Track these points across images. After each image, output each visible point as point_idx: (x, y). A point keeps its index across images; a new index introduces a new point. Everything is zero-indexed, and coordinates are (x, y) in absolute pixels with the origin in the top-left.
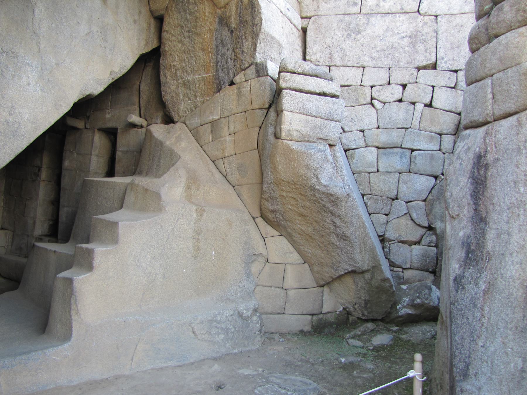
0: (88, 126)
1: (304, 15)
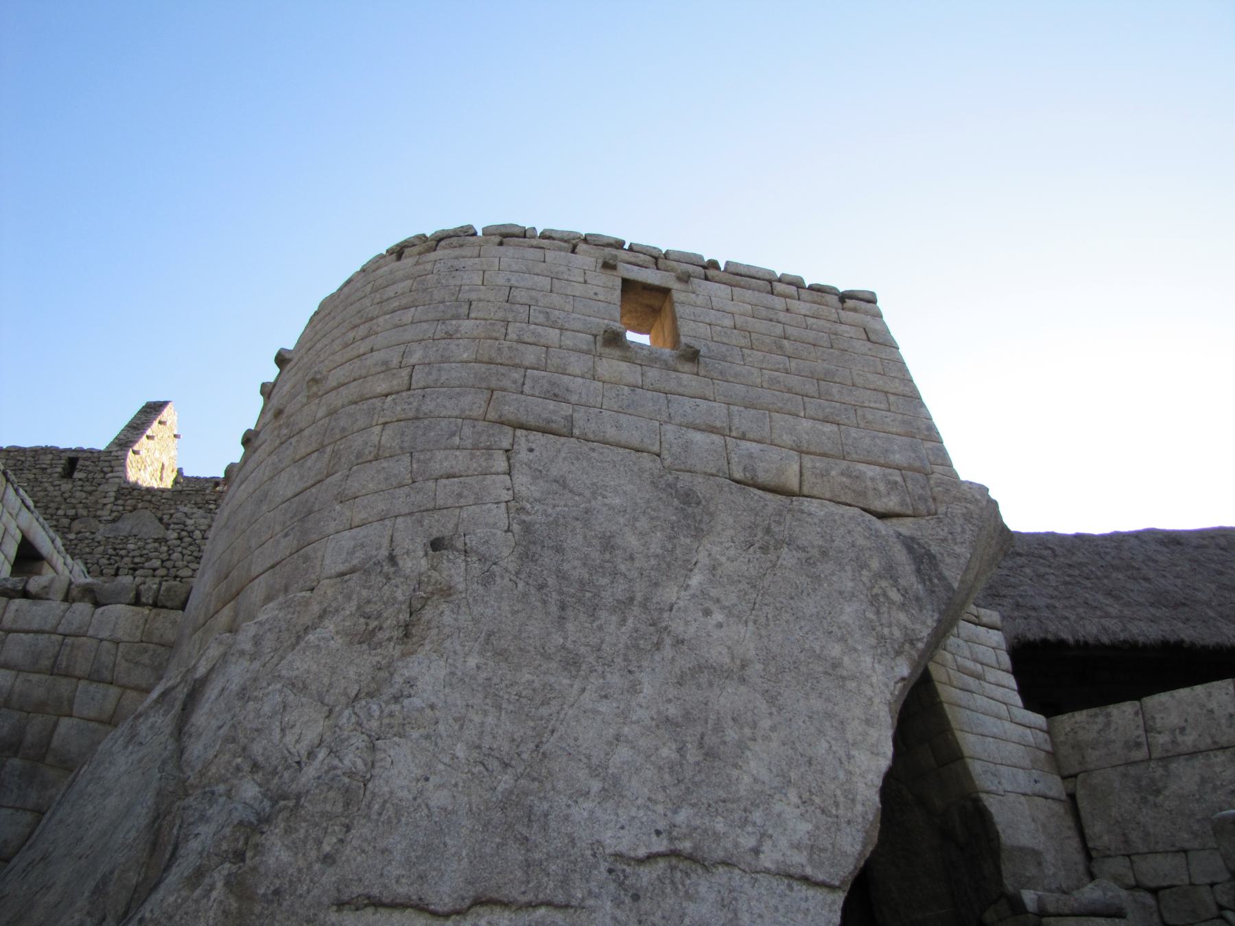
1: (1066, 773)
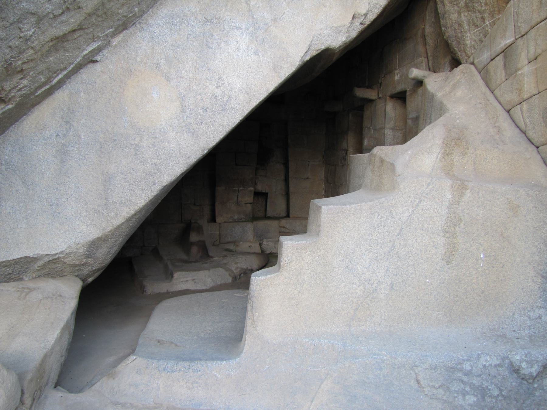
0: (381, 96)
